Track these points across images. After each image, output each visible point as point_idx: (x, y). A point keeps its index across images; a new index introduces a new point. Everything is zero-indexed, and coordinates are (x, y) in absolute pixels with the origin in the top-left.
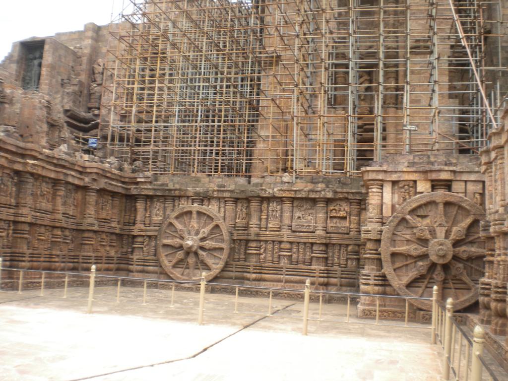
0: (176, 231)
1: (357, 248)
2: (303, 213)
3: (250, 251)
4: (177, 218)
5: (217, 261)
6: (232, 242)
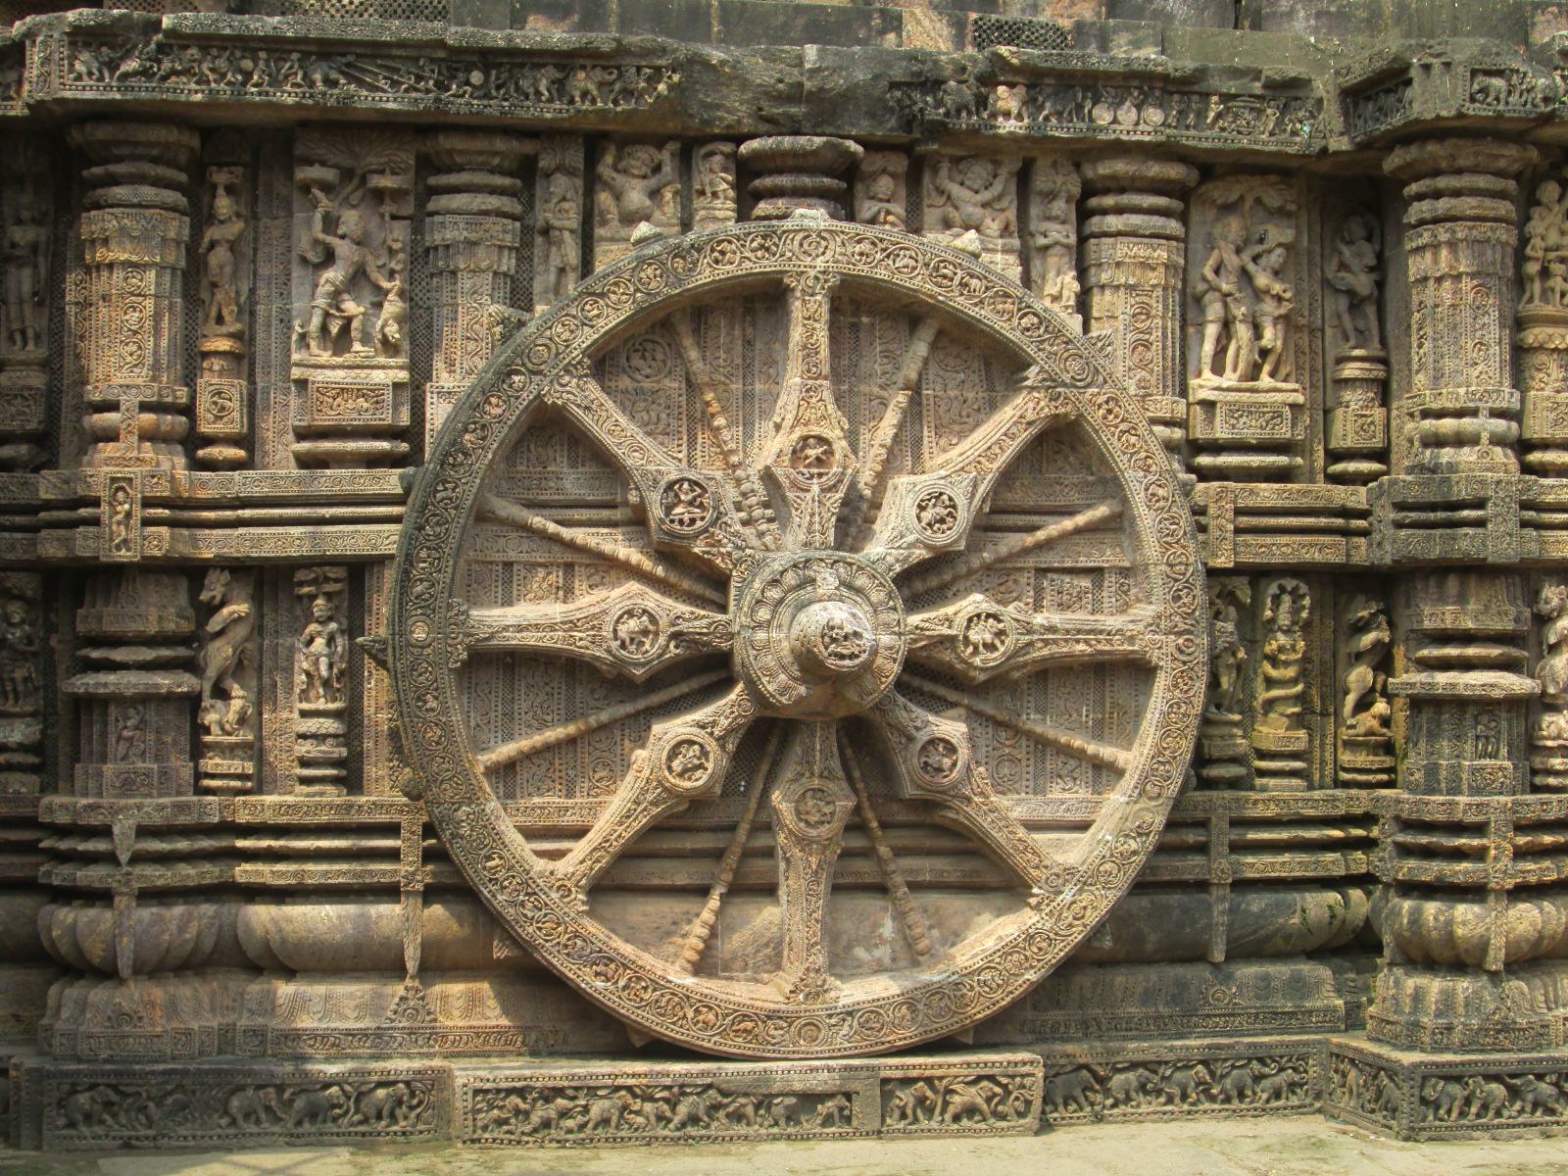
4: (604, 362)
5: (1066, 797)
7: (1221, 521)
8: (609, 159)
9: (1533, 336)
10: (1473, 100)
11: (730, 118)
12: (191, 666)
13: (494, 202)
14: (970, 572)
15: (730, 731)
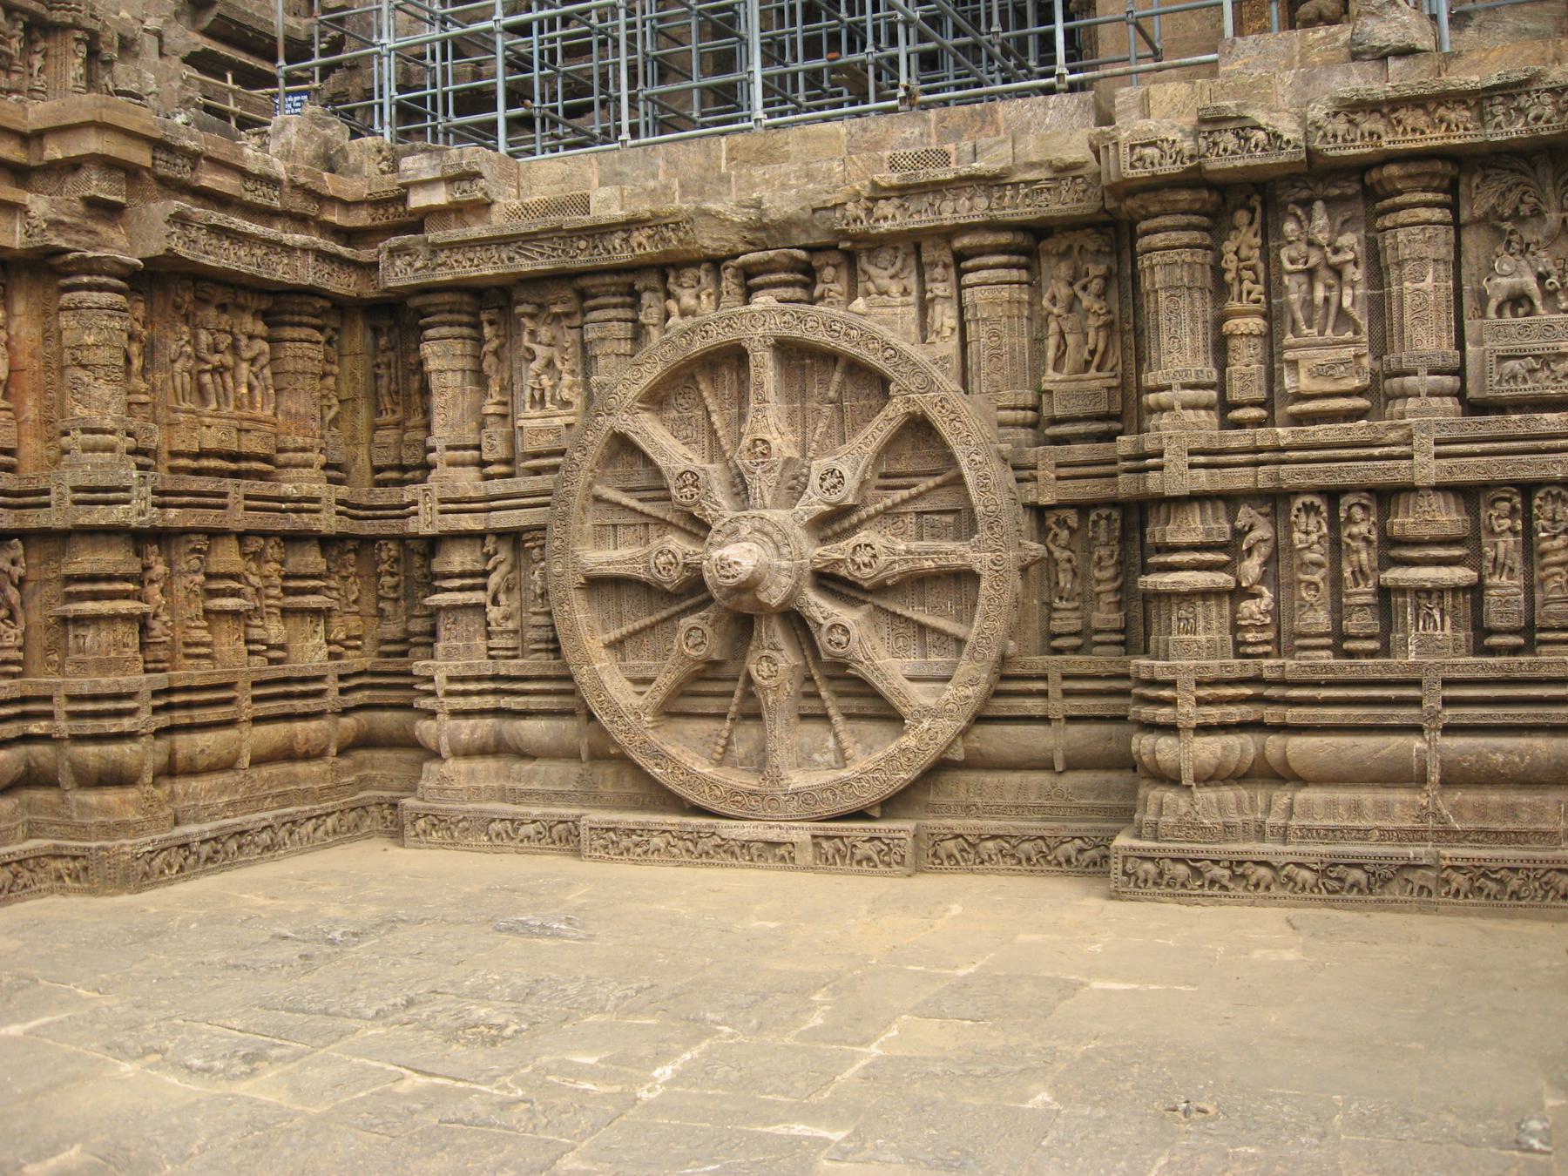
0: (658, 488)
2: (1544, 261)
3: (1166, 580)
4: (656, 399)
5: (937, 660)
6: (1026, 522)
7: (1047, 473)
8: (671, 280)
9: (1230, 325)
10: (1132, 166)
11: (728, 246)
12: (484, 588)
13: (611, 313)
14: (870, 518)
15: (716, 621)
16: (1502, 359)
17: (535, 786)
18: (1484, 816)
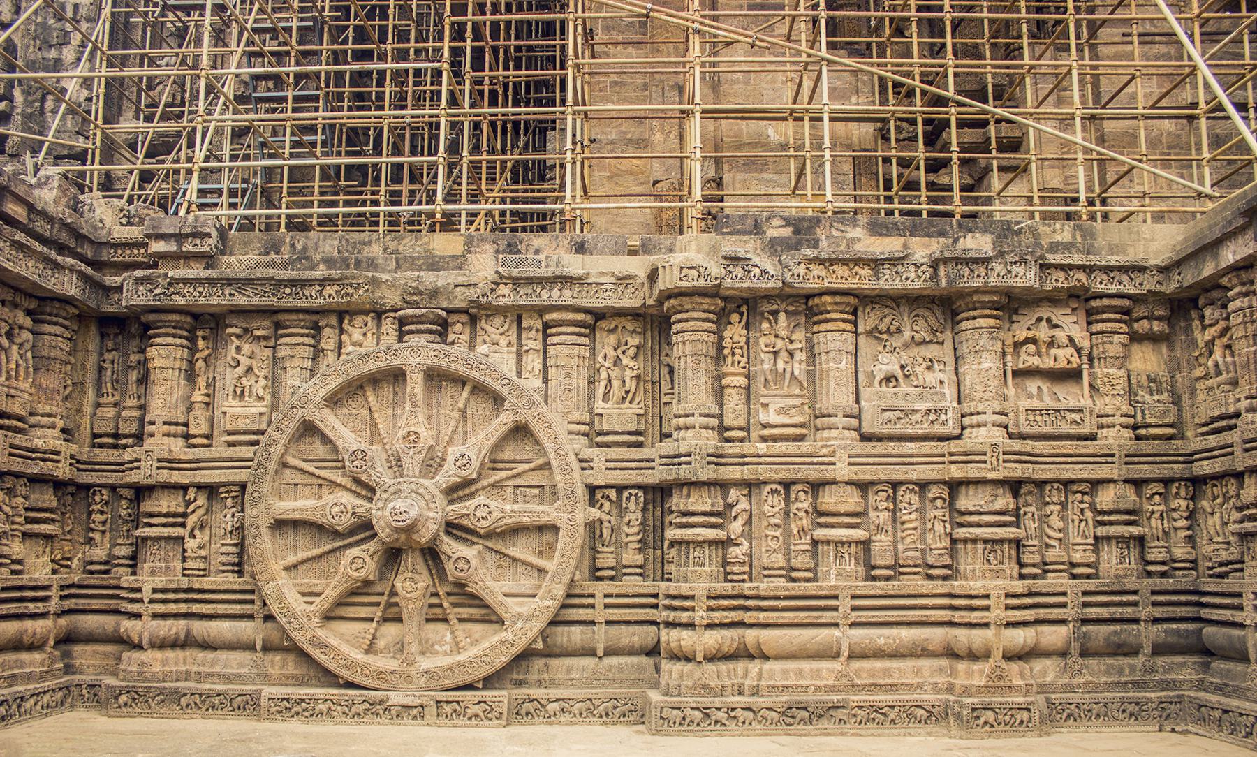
1: (1130, 492)
2: (905, 357)
4: (334, 400)
5: (526, 583)
8: (346, 321)
11: (392, 303)
12: (183, 525)
13: (300, 340)
14: (483, 488)
16: (884, 410)
17: (217, 669)
18: (873, 676)
